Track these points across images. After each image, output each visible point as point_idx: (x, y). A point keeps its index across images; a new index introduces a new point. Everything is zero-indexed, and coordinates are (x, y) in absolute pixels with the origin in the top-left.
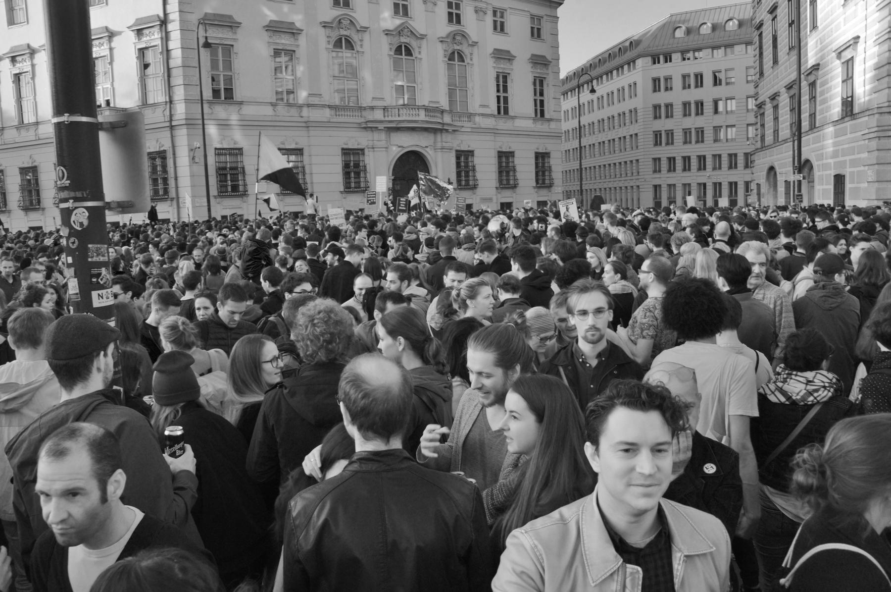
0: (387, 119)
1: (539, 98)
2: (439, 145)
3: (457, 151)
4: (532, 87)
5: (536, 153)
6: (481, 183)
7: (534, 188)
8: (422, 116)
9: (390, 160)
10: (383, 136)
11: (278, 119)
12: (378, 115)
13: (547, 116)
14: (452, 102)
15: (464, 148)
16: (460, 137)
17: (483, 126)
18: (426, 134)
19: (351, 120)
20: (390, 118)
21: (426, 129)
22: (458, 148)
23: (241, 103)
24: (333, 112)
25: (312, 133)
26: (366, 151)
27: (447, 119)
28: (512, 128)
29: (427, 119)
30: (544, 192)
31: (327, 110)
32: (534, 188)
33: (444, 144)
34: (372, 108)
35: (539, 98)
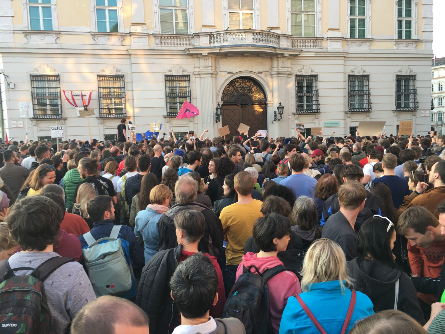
0: (212, 45)
1: (404, 18)
2: (275, 70)
3: (297, 76)
4: (396, 8)
5: (397, 76)
6: (322, 108)
7: (394, 111)
8: (249, 40)
9: (219, 85)
10: (209, 62)
11: (97, 47)
12: (204, 41)
13: (414, 37)
14: (296, 25)
15: (306, 72)
16: (304, 62)
17: (330, 50)
18: (259, 60)
19: (173, 47)
20: (216, 44)
21: (257, 55)
22: (299, 74)
23: (58, 33)
24: (158, 41)
25: (133, 60)
26: (192, 78)
27: (285, 43)
28: (368, 51)
29: (255, 43)
30: (406, 117)
31: (153, 40)
32: (394, 111)
33: (280, 69)
34: (198, 35)
35: (404, 18)
